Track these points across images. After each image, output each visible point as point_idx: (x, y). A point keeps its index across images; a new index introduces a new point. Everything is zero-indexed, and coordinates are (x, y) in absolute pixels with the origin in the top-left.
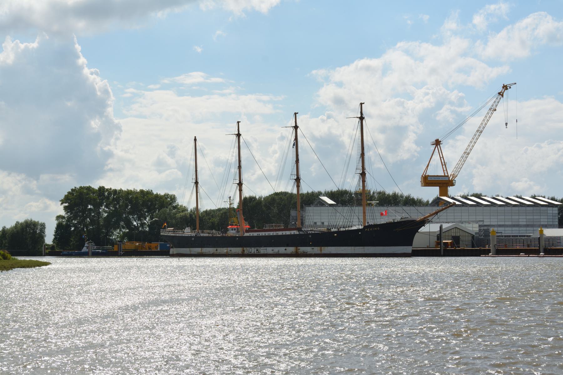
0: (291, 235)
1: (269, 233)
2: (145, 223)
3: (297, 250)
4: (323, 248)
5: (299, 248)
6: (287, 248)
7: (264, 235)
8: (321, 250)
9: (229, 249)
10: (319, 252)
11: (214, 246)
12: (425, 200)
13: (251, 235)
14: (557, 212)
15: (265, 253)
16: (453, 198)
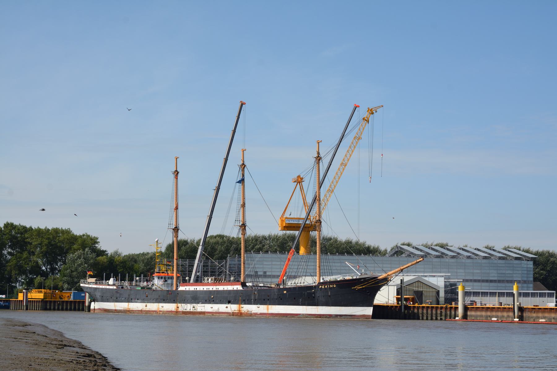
0: (233, 291)
1: (208, 287)
2: (56, 269)
3: (239, 308)
4: (270, 306)
5: (242, 306)
6: (229, 306)
7: (202, 289)
8: (268, 309)
10: (265, 311)
11: (143, 301)
12: (382, 248)
13: (187, 289)
14: (532, 266)
15: (203, 310)
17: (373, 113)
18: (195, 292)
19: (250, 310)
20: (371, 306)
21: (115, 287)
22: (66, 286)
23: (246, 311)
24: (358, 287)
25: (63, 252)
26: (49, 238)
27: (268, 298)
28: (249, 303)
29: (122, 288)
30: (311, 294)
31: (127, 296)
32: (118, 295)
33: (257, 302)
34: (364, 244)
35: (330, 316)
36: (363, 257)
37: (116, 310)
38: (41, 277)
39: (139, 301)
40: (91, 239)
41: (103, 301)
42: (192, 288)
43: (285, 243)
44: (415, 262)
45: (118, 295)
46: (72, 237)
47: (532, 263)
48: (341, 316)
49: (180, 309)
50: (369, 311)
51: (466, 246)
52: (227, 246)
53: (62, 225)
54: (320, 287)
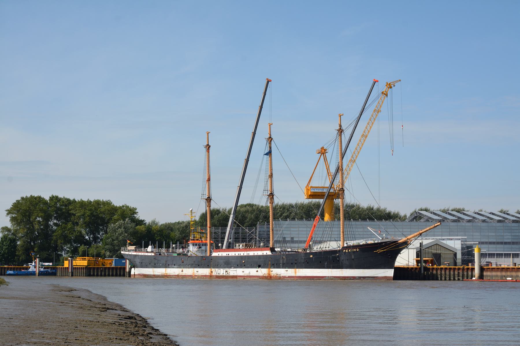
1: (239, 253)
2: (98, 238)
3: (269, 272)
4: (297, 270)
6: (259, 270)
8: (295, 273)
10: (293, 275)
11: (179, 266)
12: (402, 214)
13: (220, 255)
16: (435, 214)
17: (391, 88)
18: (228, 257)
19: (279, 273)
21: (153, 254)
22: (108, 253)
23: (275, 275)
24: (380, 251)
25: (105, 223)
26: (91, 210)
27: (296, 262)
28: (278, 267)
29: (160, 254)
30: (336, 257)
31: (164, 262)
32: (156, 262)
34: (385, 210)
35: (354, 278)
36: (384, 222)
37: (154, 275)
38: (85, 245)
39: (175, 266)
40: (130, 210)
41: (142, 267)
42: (224, 254)
43: (312, 211)
44: (433, 226)
45: (156, 262)
46: (113, 209)
48: (364, 277)
49: (214, 274)
50: (390, 273)
51: (481, 211)
52: (257, 214)
53: (103, 197)
54: (344, 251)
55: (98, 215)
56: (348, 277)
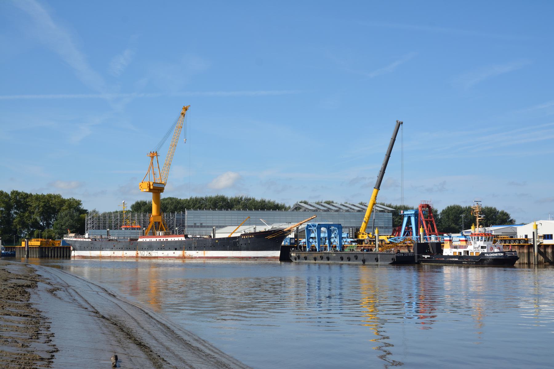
0: (179, 241)
4: (206, 252)
6: (176, 252)
8: (204, 254)
9: (125, 252)
10: (203, 255)
11: (112, 249)
12: (287, 205)
14: (391, 216)
18: (151, 242)
19: (191, 255)
20: (278, 250)
21: (90, 240)
22: (57, 236)
26: (44, 202)
30: (236, 242)
31: (99, 246)
32: (92, 246)
33: (197, 248)
34: (274, 202)
35: (250, 258)
40: (76, 202)
41: (81, 250)
42: (148, 240)
43: (218, 203)
45: (92, 246)
47: (391, 214)
48: (257, 257)
49: (140, 255)
50: (277, 254)
52: (175, 205)
55: (50, 206)
56: (245, 257)
